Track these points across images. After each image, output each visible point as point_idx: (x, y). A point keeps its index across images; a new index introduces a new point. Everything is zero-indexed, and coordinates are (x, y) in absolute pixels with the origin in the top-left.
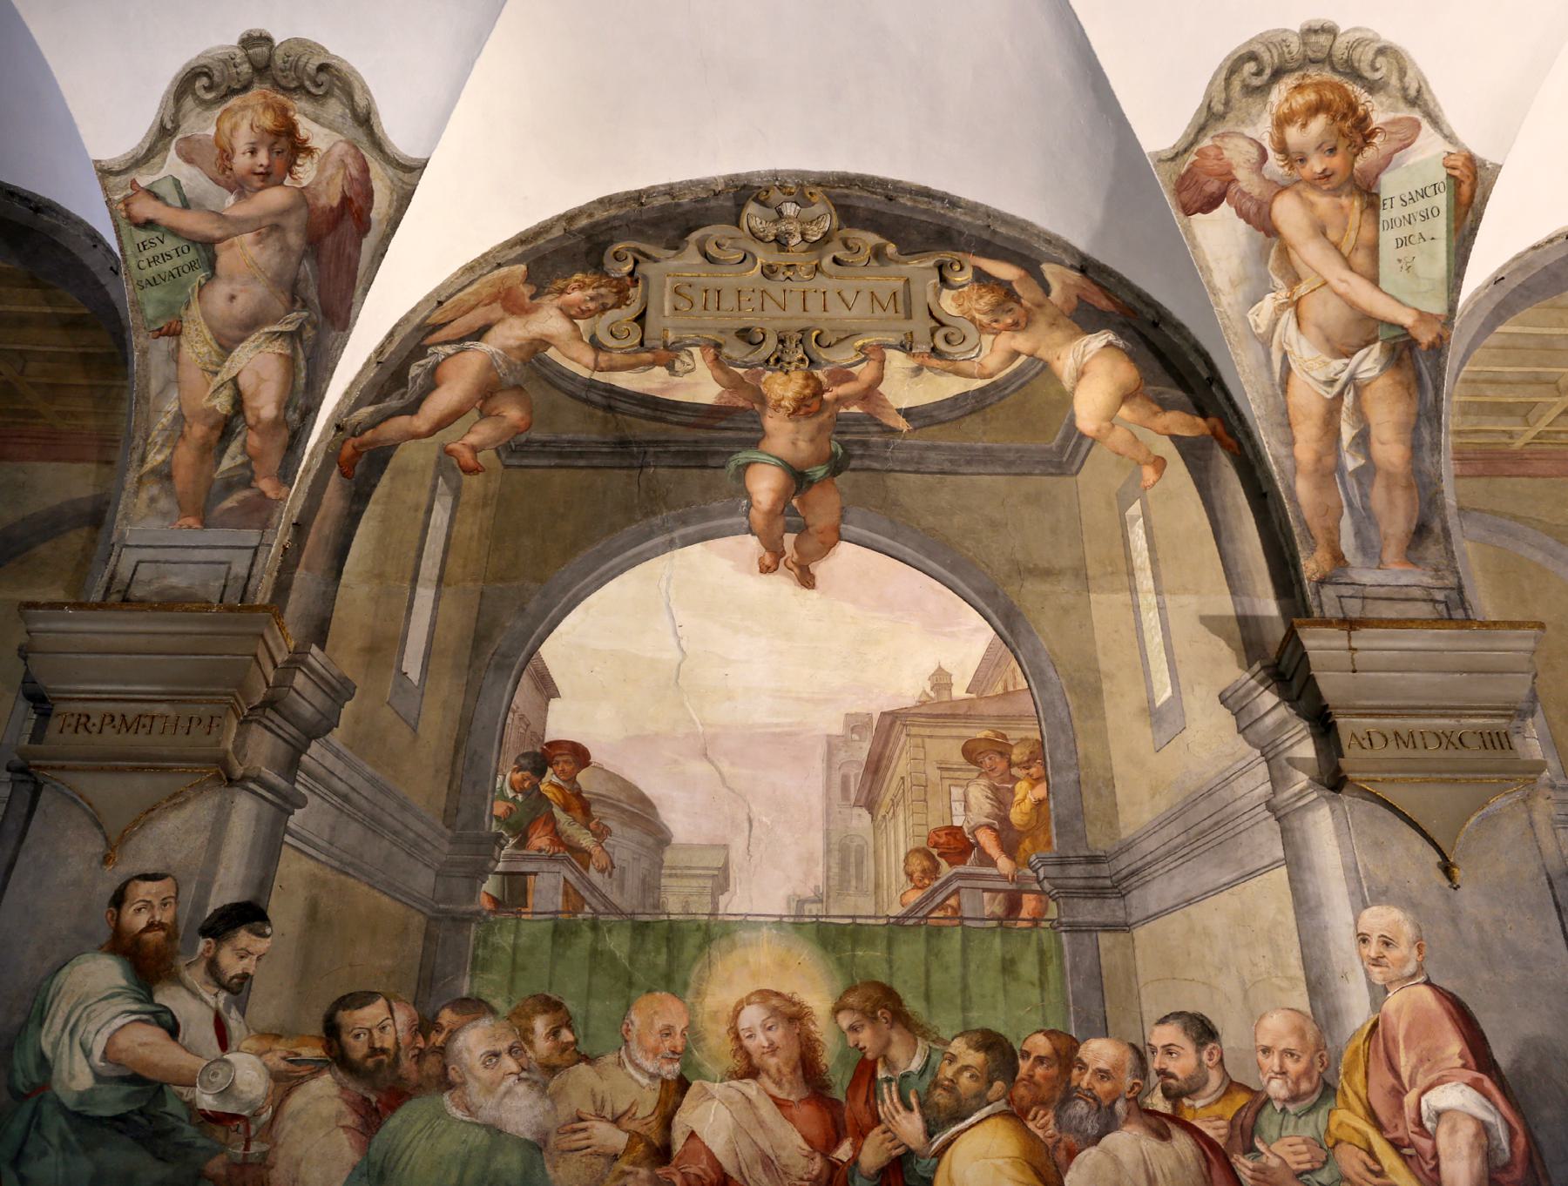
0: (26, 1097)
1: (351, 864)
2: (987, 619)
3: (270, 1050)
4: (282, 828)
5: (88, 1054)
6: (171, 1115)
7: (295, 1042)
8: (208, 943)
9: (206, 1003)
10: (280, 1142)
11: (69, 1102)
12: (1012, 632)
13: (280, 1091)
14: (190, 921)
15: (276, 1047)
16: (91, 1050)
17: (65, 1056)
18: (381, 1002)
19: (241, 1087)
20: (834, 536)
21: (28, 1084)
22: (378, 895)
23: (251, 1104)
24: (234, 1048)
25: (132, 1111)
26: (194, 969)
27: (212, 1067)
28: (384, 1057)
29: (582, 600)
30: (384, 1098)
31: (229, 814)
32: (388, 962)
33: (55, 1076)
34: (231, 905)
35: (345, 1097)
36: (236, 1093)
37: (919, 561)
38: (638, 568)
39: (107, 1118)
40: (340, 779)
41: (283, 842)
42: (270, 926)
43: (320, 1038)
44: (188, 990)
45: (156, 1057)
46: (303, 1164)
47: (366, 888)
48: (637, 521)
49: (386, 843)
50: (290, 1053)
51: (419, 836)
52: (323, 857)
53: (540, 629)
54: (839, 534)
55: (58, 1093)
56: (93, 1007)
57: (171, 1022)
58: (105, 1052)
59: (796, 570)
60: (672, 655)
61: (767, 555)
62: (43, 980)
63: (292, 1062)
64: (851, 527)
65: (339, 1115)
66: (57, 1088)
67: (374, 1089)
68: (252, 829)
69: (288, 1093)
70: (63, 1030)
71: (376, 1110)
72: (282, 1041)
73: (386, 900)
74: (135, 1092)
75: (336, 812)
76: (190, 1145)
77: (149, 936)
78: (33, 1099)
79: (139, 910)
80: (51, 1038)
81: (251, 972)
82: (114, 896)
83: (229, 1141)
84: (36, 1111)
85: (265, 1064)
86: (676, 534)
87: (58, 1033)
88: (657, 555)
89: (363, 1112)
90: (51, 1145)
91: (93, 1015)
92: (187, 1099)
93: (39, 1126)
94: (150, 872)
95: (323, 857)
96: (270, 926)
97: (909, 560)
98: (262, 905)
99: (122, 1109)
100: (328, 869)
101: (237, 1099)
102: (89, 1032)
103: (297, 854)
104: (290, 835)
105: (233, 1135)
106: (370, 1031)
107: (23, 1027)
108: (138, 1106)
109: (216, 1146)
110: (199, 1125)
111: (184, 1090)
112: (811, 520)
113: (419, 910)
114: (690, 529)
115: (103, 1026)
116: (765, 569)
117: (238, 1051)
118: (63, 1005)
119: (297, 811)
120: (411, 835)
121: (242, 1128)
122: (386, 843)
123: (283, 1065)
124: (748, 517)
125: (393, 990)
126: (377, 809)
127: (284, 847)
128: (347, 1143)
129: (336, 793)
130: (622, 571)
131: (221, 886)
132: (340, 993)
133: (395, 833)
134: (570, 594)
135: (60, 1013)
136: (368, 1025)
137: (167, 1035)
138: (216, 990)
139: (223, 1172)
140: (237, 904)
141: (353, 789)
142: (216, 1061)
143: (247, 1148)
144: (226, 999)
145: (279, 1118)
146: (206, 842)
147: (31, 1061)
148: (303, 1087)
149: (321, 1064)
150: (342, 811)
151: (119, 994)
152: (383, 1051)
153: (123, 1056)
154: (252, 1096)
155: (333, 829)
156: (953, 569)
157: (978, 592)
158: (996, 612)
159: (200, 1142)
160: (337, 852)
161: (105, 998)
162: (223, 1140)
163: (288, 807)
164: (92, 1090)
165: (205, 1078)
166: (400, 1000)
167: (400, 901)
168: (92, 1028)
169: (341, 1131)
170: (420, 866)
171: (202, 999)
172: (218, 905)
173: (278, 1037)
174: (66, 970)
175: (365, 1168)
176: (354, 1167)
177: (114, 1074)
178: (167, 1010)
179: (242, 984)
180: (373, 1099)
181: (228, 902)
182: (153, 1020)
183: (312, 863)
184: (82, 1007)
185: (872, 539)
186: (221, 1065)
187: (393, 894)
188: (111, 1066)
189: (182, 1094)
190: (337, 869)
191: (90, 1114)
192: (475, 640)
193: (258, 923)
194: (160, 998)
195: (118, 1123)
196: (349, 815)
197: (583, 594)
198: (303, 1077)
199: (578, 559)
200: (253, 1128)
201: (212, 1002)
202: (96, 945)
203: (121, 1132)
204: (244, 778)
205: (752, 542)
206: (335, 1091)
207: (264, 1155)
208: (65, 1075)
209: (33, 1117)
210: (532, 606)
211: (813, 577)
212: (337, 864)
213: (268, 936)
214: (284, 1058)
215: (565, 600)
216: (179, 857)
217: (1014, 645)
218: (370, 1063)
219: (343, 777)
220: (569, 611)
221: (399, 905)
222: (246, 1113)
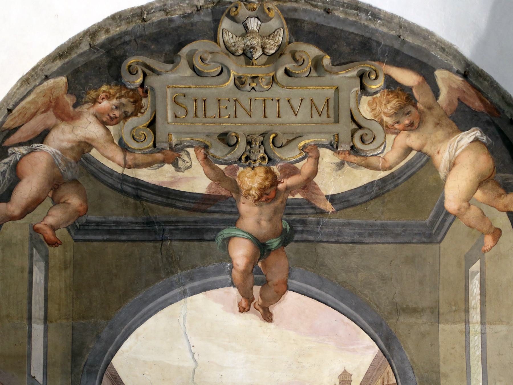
2: (375, 340)
12: (389, 349)
20: (284, 287)
29: (134, 330)
37: (335, 303)
38: (166, 310)
48: (162, 279)
53: (111, 349)
54: (287, 286)
59: (261, 310)
60: (190, 364)
61: (243, 300)
64: (295, 282)
86: (187, 287)
88: (176, 301)
97: (330, 303)
112: (269, 277)
114: (196, 284)
116: (243, 310)
124: (231, 275)
130: (156, 312)
134: (126, 326)
156: (356, 310)
157: (370, 324)
158: (380, 336)
185: (307, 289)
192: (72, 357)
197: (134, 327)
199: (129, 304)
205: (234, 292)
210: (104, 335)
211: (271, 315)
215: (123, 330)
217: (390, 357)
220: (127, 338)
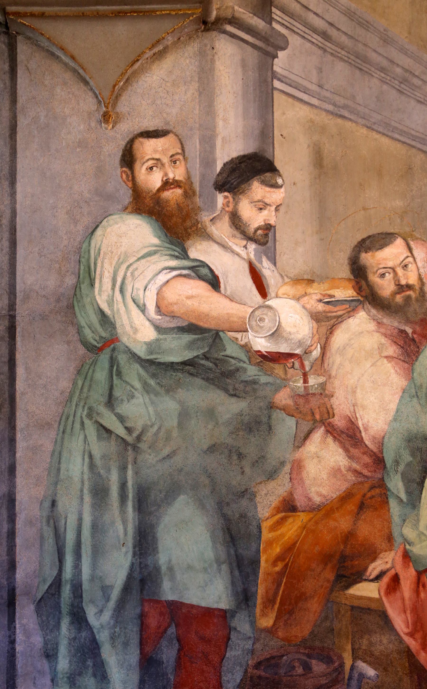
0: (101, 349)
1: (345, 107)
3: (306, 294)
4: (270, 74)
5: (143, 309)
6: (233, 358)
7: (326, 285)
8: (226, 197)
9: (238, 255)
10: (333, 373)
11: (141, 351)
13: (323, 330)
14: (203, 177)
15: (310, 290)
16: (144, 305)
17: (122, 310)
18: (399, 241)
19: (288, 329)
21: (97, 338)
22: (377, 136)
23: (300, 343)
24: (273, 295)
25: (197, 357)
26: (219, 224)
27: (257, 313)
28: (410, 293)
30: (418, 328)
31: (213, 61)
32: (399, 203)
33: (119, 330)
34: (237, 158)
35: (383, 330)
36: (284, 334)
39: (177, 363)
40: (315, 13)
41: (273, 89)
42: (280, 176)
43: (349, 280)
44: (218, 243)
45: (205, 308)
46: (358, 391)
47: (364, 131)
49: (375, 82)
50: (324, 295)
51: (406, 71)
52: (315, 101)
55: (128, 344)
56: (135, 266)
57: (210, 275)
58: (158, 306)
62: (81, 243)
63: (328, 303)
65: (381, 347)
66: (125, 340)
67: (408, 321)
68: (240, 77)
69: (331, 331)
70: (113, 289)
71: (413, 340)
72: (315, 284)
73: (385, 140)
74: (198, 339)
75: (320, 52)
76: (254, 382)
77: (167, 194)
78: (107, 351)
79: (151, 168)
80: (105, 297)
81: (272, 222)
82: (124, 156)
83: (288, 376)
84: (113, 361)
85: (304, 307)
87: (111, 293)
89: (402, 343)
90: (136, 390)
91: (136, 273)
92: (243, 343)
93: (119, 374)
94: (151, 129)
95: (315, 101)
96: (280, 176)
98: (268, 155)
99: (188, 355)
100: (324, 113)
101: (287, 340)
102: (138, 289)
103: (290, 100)
104: (279, 80)
105: (291, 371)
106: (393, 269)
107: (77, 287)
108: (202, 351)
109: (278, 381)
110: (258, 364)
111: (239, 335)
113: (420, 150)
115: (149, 282)
117: (277, 297)
118: (106, 265)
119: (280, 54)
120: (398, 70)
121: (297, 365)
122: (375, 82)
123: (321, 307)
125: (407, 229)
126: (360, 45)
127: (275, 93)
128: (393, 371)
129: (315, 30)
131: (223, 138)
132: (359, 237)
133: (382, 70)
135: (106, 274)
136: (390, 264)
137: (210, 287)
138: (244, 242)
139: (290, 402)
140: (244, 156)
141: (331, 24)
142: (260, 307)
143: (305, 381)
144: (255, 250)
145: (328, 354)
146: (196, 94)
147: (94, 319)
148: (344, 326)
149: (354, 304)
150: (325, 51)
151: (155, 252)
152: (409, 287)
153: (175, 308)
154: (300, 336)
155: (320, 70)
159: (263, 379)
160: (328, 94)
161: (143, 257)
162: (283, 376)
163: (270, 49)
164: (157, 340)
165: (254, 323)
166: (416, 239)
167: (399, 141)
168: (140, 285)
169: (385, 361)
170: (413, 103)
171: (233, 252)
172: (227, 159)
173: (310, 282)
174: (99, 232)
175: (413, 391)
176: (404, 391)
177: (172, 325)
178: (204, 265)
179: (266, 235)
180: (409, 331)
181: (235, 155)
182: (193, 274)
183: (306, 108)
184: (124, 267)
186: (265, 310)
187: (390, 134)
188: (168, 319)
189: (237, 339)
190: (332, 113)
191: (162, 360)
193: (268, 174)
194: (193, 254)
195: (187, 367)
196: (332, 54)
198: (341, 316)
200: (307, 364)
201: (243, 253)
202: (120, 207)
203: (192, 374)
204: (219, 21)
206: (372, 326)
207: (323, 386)
208: (128, 328)
209: (112, 366)
212: (330, 108)
213: (281, 187)
214: (320, 301)
216: (174, 111)
218: (399, 299)
219: (319, 11)
221: (399, 145)
222: (297, 352)
